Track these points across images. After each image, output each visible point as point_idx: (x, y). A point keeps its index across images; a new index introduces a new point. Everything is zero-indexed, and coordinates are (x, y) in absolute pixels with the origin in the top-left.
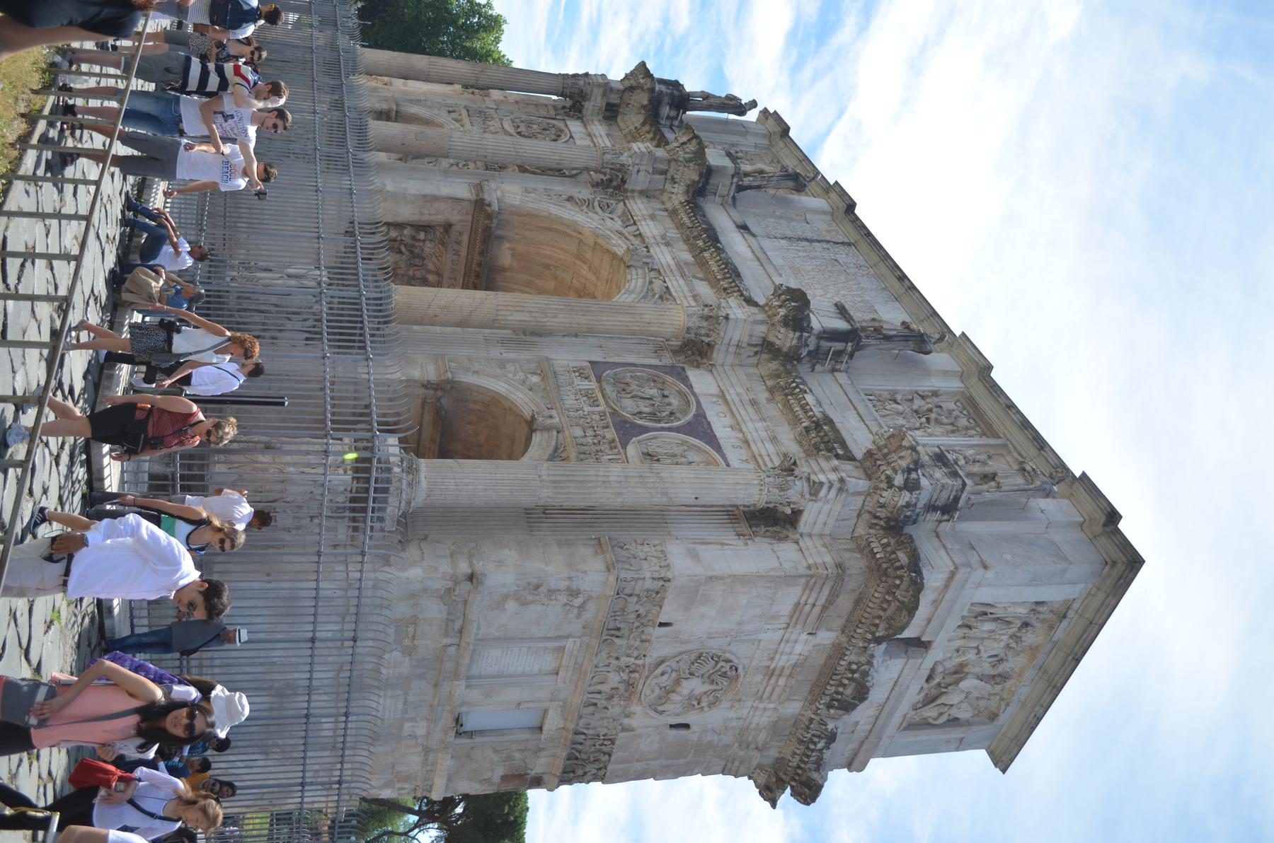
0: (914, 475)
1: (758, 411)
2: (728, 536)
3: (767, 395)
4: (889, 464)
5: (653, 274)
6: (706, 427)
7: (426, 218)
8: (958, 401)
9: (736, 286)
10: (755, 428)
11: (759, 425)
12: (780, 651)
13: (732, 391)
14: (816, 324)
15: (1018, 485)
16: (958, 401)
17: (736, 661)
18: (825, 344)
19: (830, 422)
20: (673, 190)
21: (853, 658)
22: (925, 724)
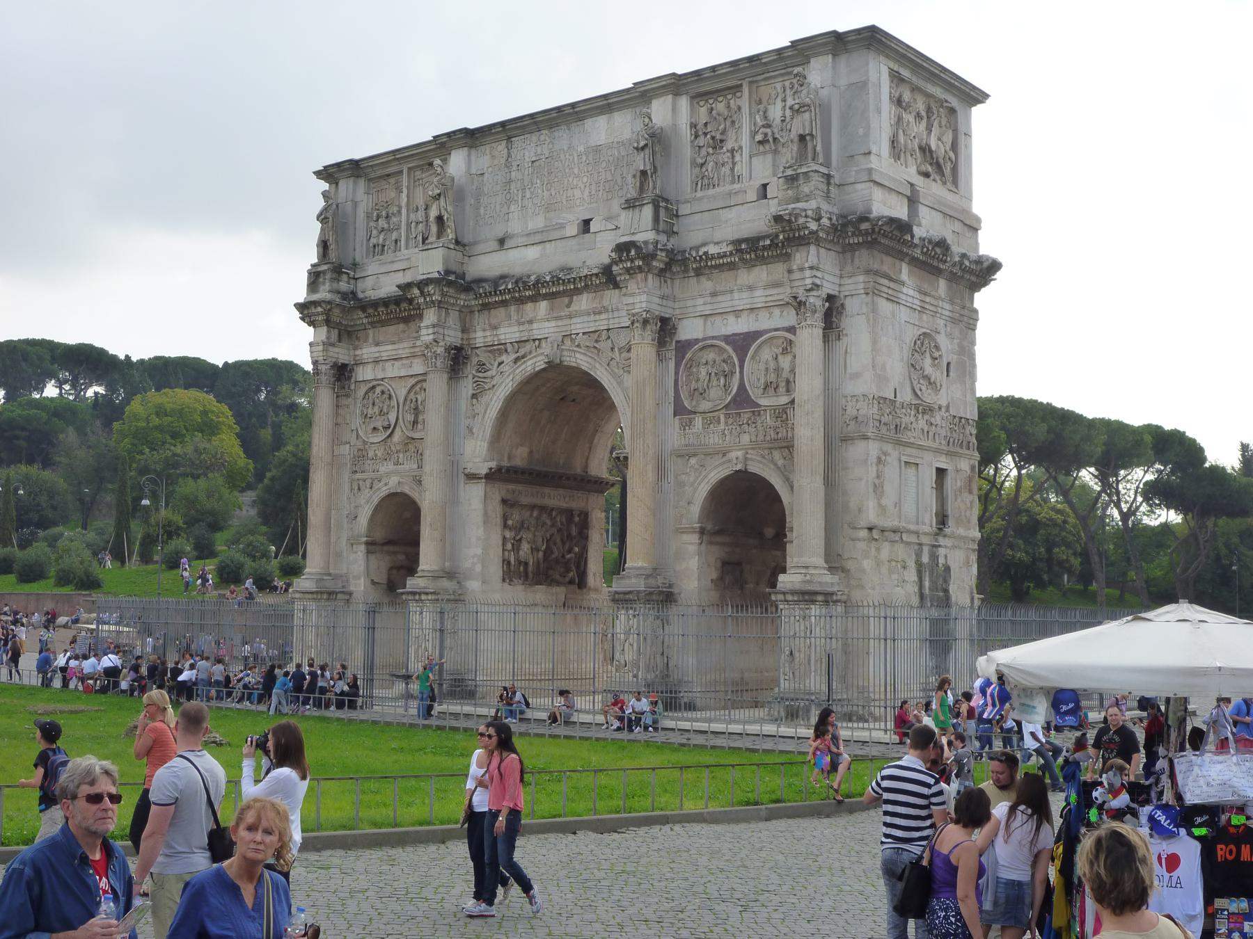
0: (810, 213)
1: (723, 293)
2: (840, 346)
3: (703, 279)
4: (799, 230)
5: (568, 342)
6: (737, 338)
7: (499, 520)
8: (698, 103)
9: (586, 276)
10: (741, 300)
11: (736, 295)
12: (911, 305)
13: (699, 309)
14: (650, 236)
15: (811, 118)
16: (698, 103)
17: (916, 337)
18: (662, 226)
19: (737, 242)
20: (462, 304)
21: (919, 252)
22: (955, 170)
